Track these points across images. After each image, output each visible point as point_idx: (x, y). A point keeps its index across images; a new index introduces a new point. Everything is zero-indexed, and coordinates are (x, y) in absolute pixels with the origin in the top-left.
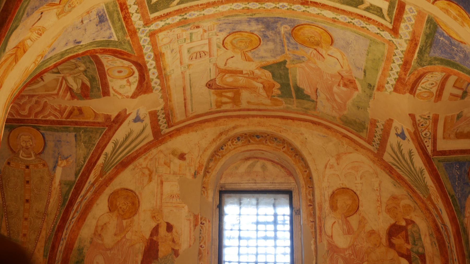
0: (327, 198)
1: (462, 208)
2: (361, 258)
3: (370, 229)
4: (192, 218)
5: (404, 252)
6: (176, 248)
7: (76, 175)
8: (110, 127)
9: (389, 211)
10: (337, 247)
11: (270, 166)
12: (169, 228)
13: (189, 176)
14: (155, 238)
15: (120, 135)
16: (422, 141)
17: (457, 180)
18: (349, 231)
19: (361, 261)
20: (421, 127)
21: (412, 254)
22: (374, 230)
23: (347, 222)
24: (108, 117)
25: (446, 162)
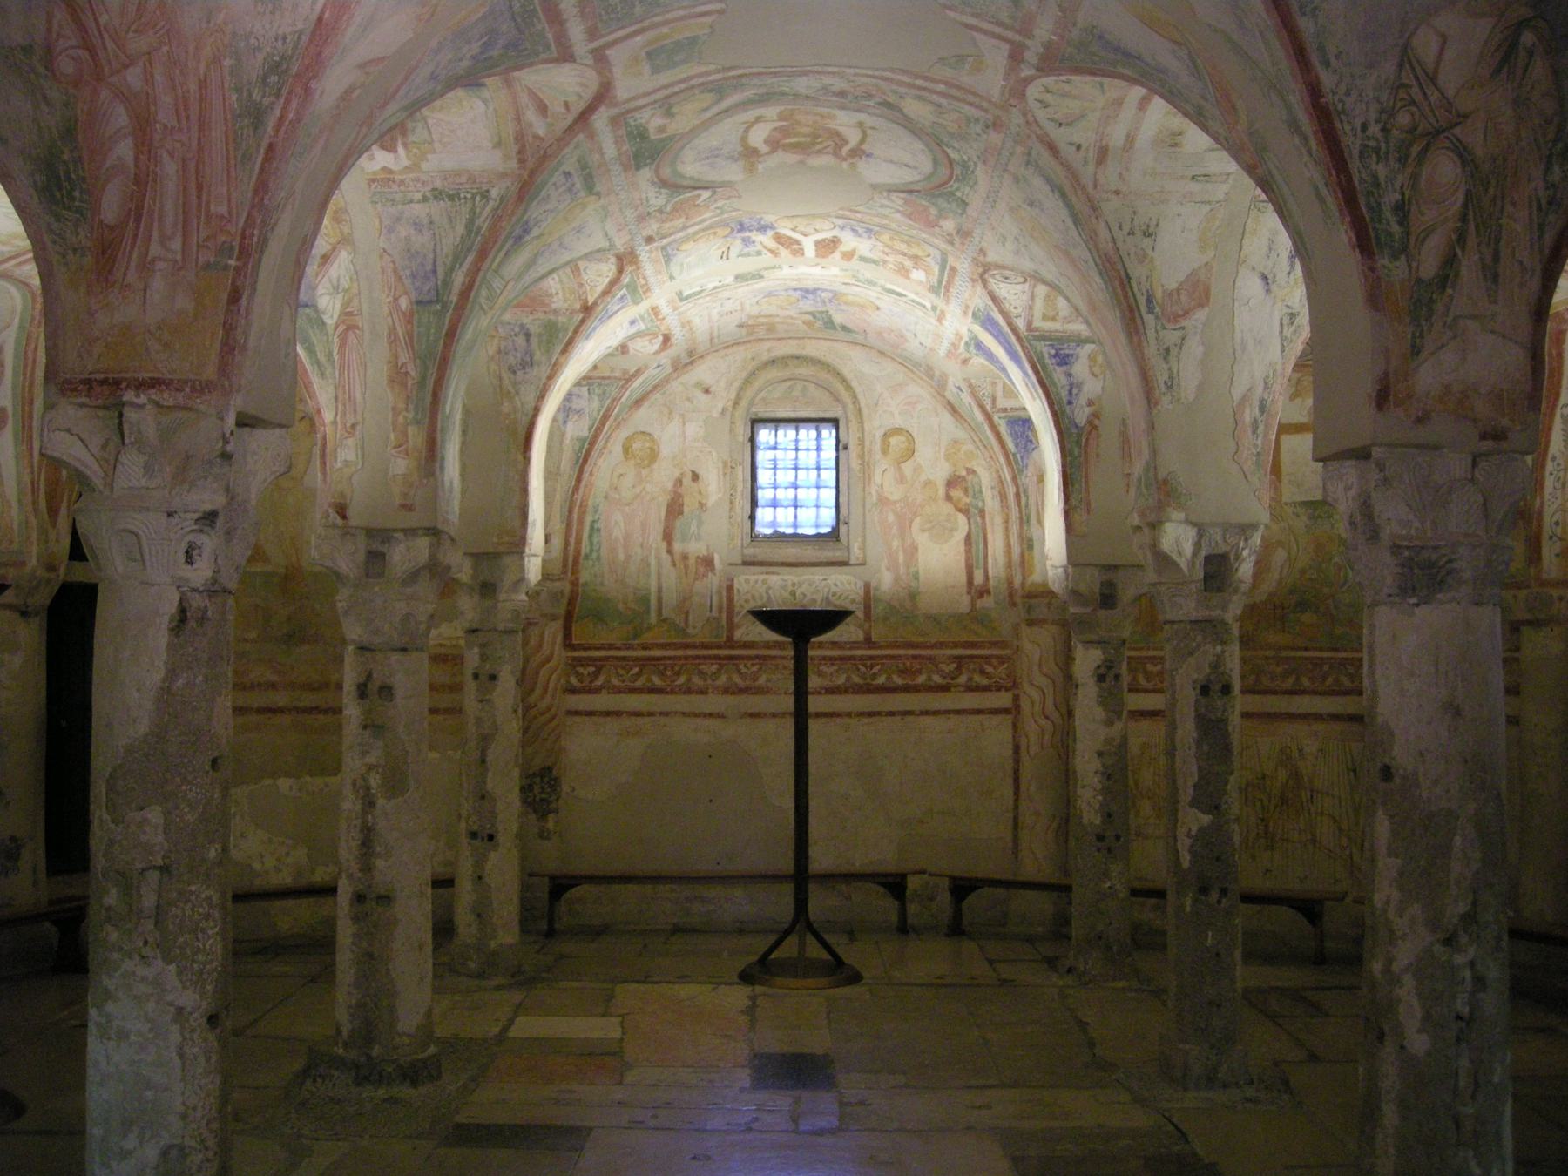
0: (878, 440)
4: (721, 465)
5: (962, 505)
6: (704, 501)
7: (590, 429)
8: (628, 381)
9: (948, 457)
11: (812, 387)
12: (695, 477)
13: (715, 414)
14: (679, 491)
15: (637, 382)
18: (902, 479)
23: (900, 468)
24: (625, 372)
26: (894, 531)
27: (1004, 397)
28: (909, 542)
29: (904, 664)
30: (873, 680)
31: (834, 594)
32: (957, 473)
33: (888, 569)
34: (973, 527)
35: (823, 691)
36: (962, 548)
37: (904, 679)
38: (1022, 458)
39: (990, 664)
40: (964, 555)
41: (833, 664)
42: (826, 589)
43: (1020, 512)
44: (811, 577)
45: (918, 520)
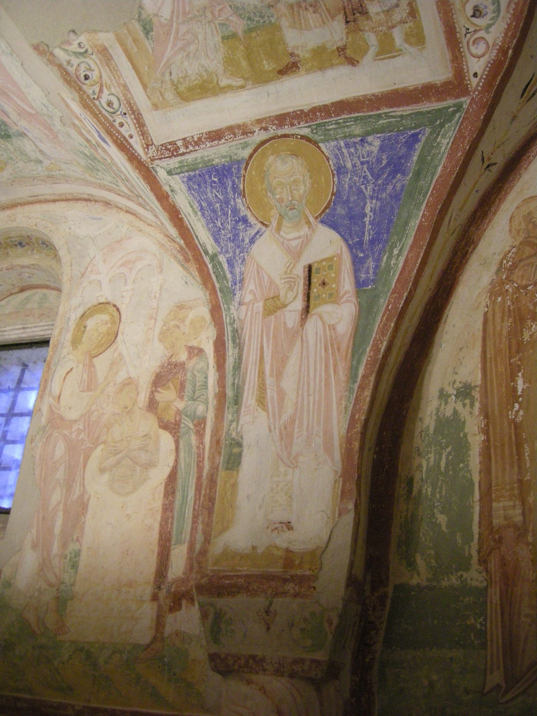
1: (235, 284)
2: (96, 435)
3: (126, 376)
5: (170, 417)
10: (62, 418)
16: (112, 125)
17: (220, 214)
19: (94, 444)
20: (87, 82)
21: (183, 421)
22: (130, 378)
25: (187, 171)
26: (60, 475)
27: (156, 107)
32: (173, 360)
36: (159, 502)
38: (230, 262)
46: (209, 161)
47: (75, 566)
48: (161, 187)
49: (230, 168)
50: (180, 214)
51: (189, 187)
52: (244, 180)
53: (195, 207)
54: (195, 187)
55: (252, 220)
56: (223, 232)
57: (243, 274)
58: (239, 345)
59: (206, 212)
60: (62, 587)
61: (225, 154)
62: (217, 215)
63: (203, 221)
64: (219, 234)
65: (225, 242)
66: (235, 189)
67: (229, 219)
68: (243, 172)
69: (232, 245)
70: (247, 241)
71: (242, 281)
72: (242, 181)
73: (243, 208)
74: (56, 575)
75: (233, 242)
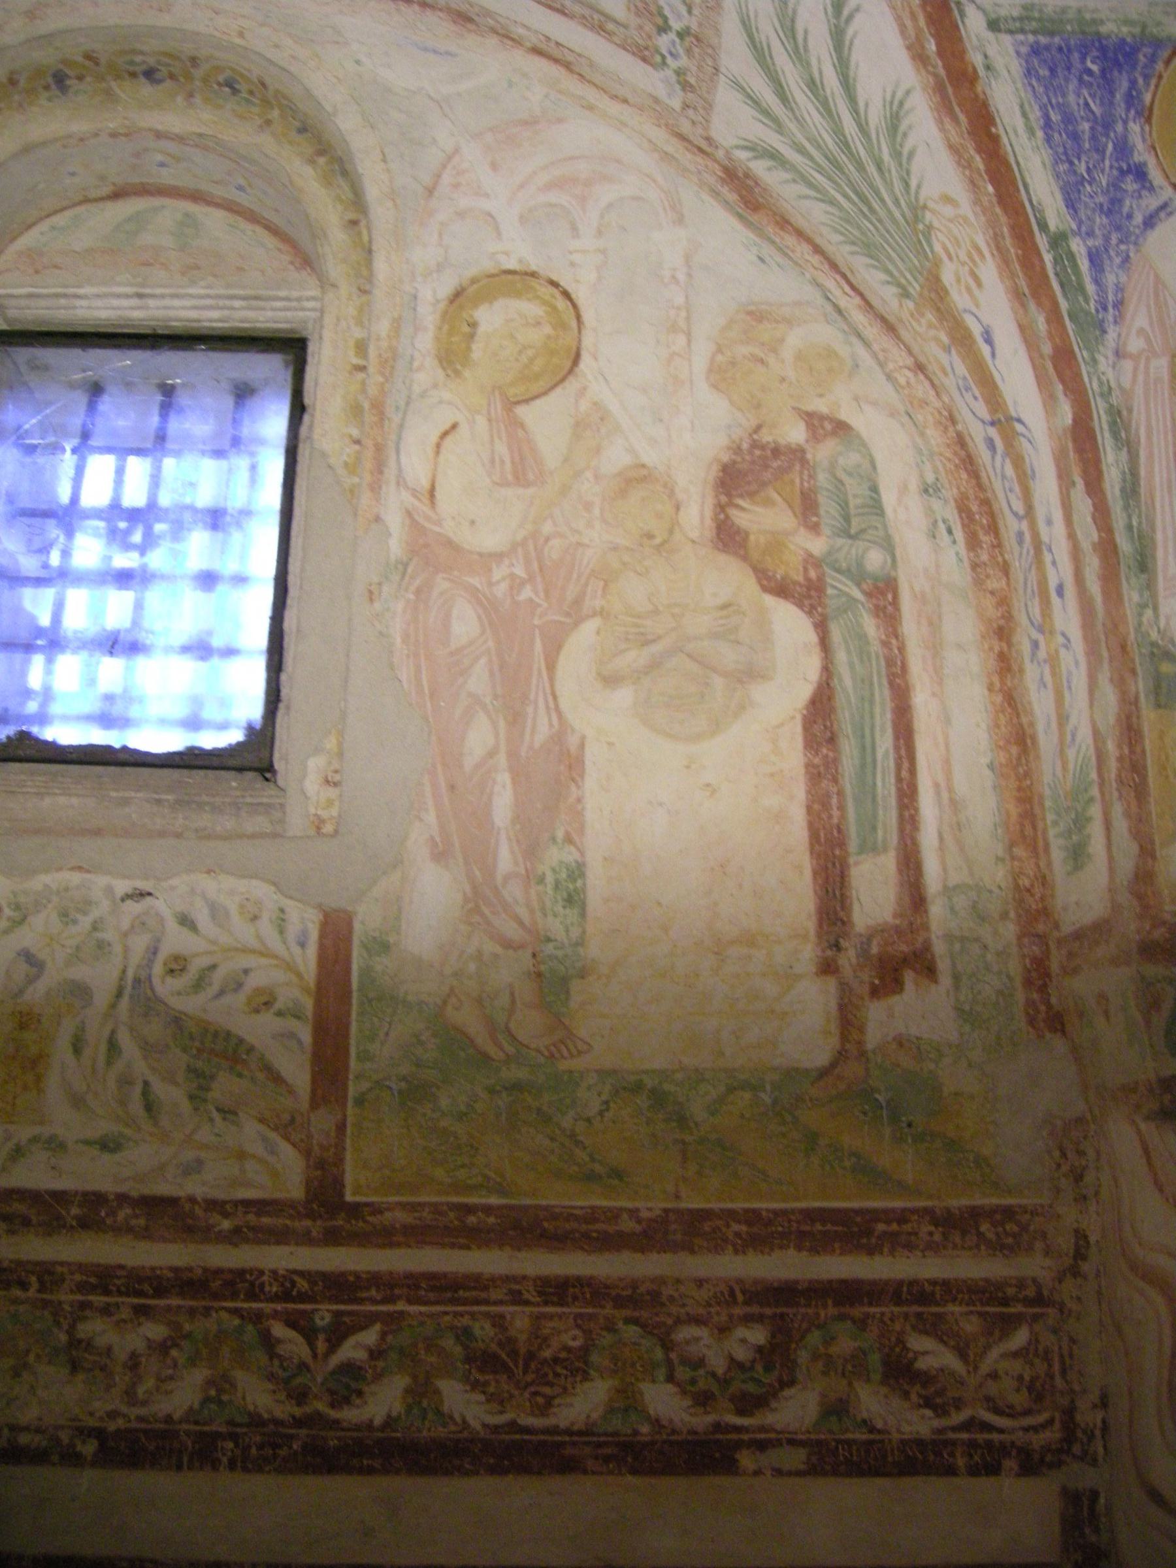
0: (429, 315)
1: (1105, 309)
2: (570, 595)
3: (626, 460)
5: (791, 568)
17: (1087, 146)
19: (568, 615)
21: (829, 580)
22: (643, 466)
23: (516, 424)
25: (1034, 32)
26: (478, 681)
28: (542, 729)
29: (499, 1321)
30: (341, 1400)
31: (177, 965)
32: (766, 437)
33: (441, 855)
34: (841, 657)
35: (89, 1448)
37: (499, 1401)
38: (1095, 259)
39: (935, 1328)
40: (800, 792)
41: (142, 1312)
42: (140, 944)
43: (1101, 513)
44: (76, 878)
45: (585, 637)
46: (1094, 21)
47: (574, 899)
48: (963, 52)
49: (1135, 50)
50: (995, 125)
51: (1029, 71)
52: (1157, 86)
53: (1032, 117)
54: (1041, 72)
55: (1155, 175)
56: (1088, 188)
57: (1122, 290)
58: (1129, 445)
59: (1056, 135)
60: (549, 948)
61: (1135, 17)
62: (1080, 147)
63: (1046, 154)
64: (1079, 191)
65: (1089, 213)
66: (1131, 99)
67: (1107, 163)
68: (1160, 66)
69: (1105, 220)
70: (1138, 219)
71: (1119, 304)
72: (1152, 87)
73: (1140, 146)
74: (521, 923)
75: (1107, 216)
